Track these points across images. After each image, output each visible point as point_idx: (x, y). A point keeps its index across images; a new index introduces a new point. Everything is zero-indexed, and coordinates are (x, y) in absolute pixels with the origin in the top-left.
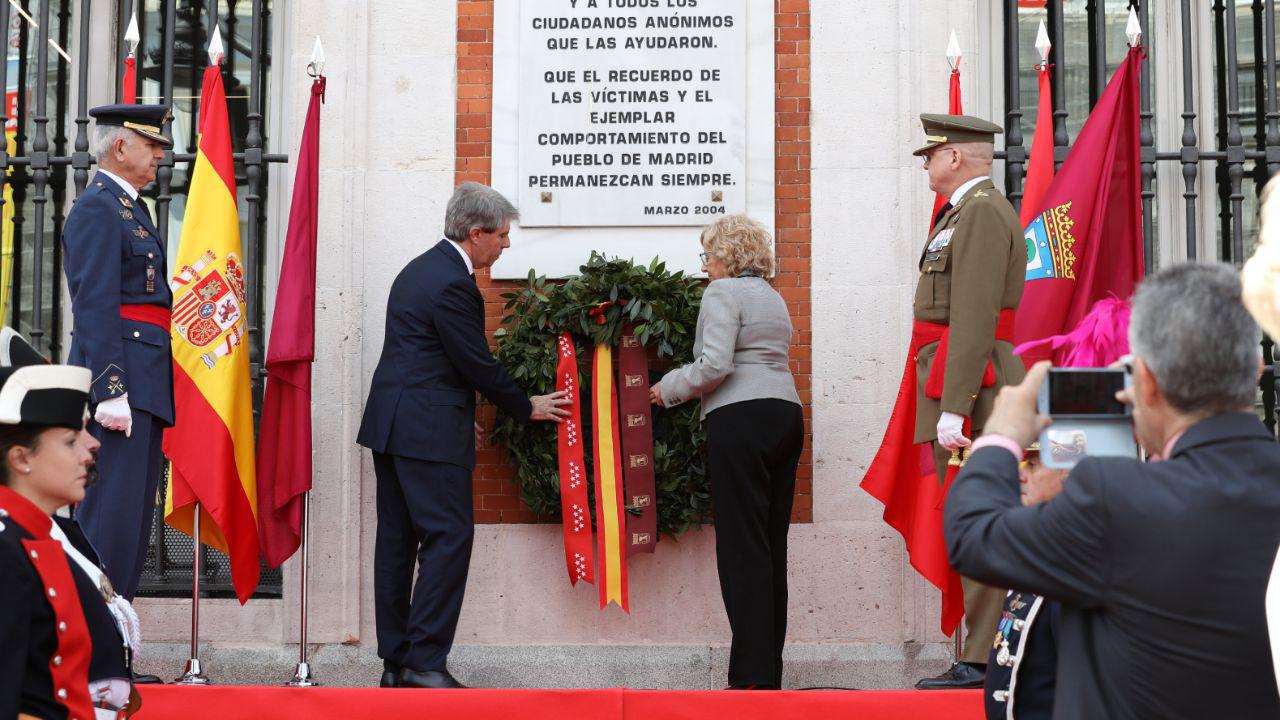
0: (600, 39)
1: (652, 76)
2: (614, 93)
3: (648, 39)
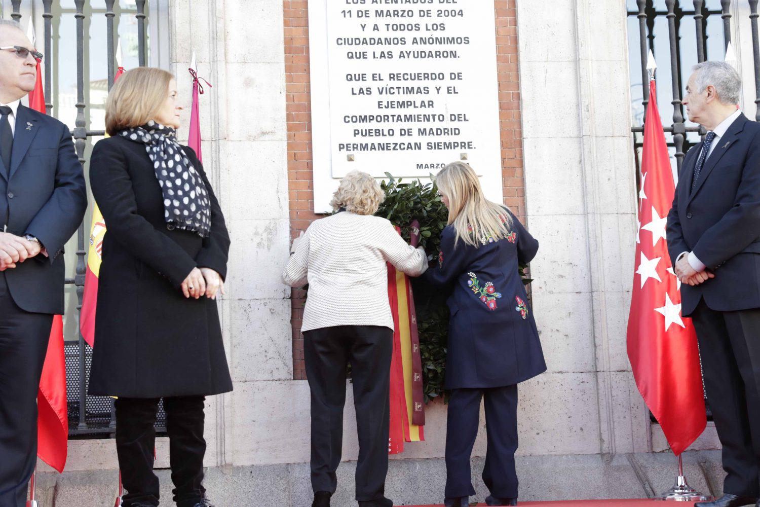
0: (383, 52)
1: (418, 76)
2: (393, 88)
3: (414, 52)
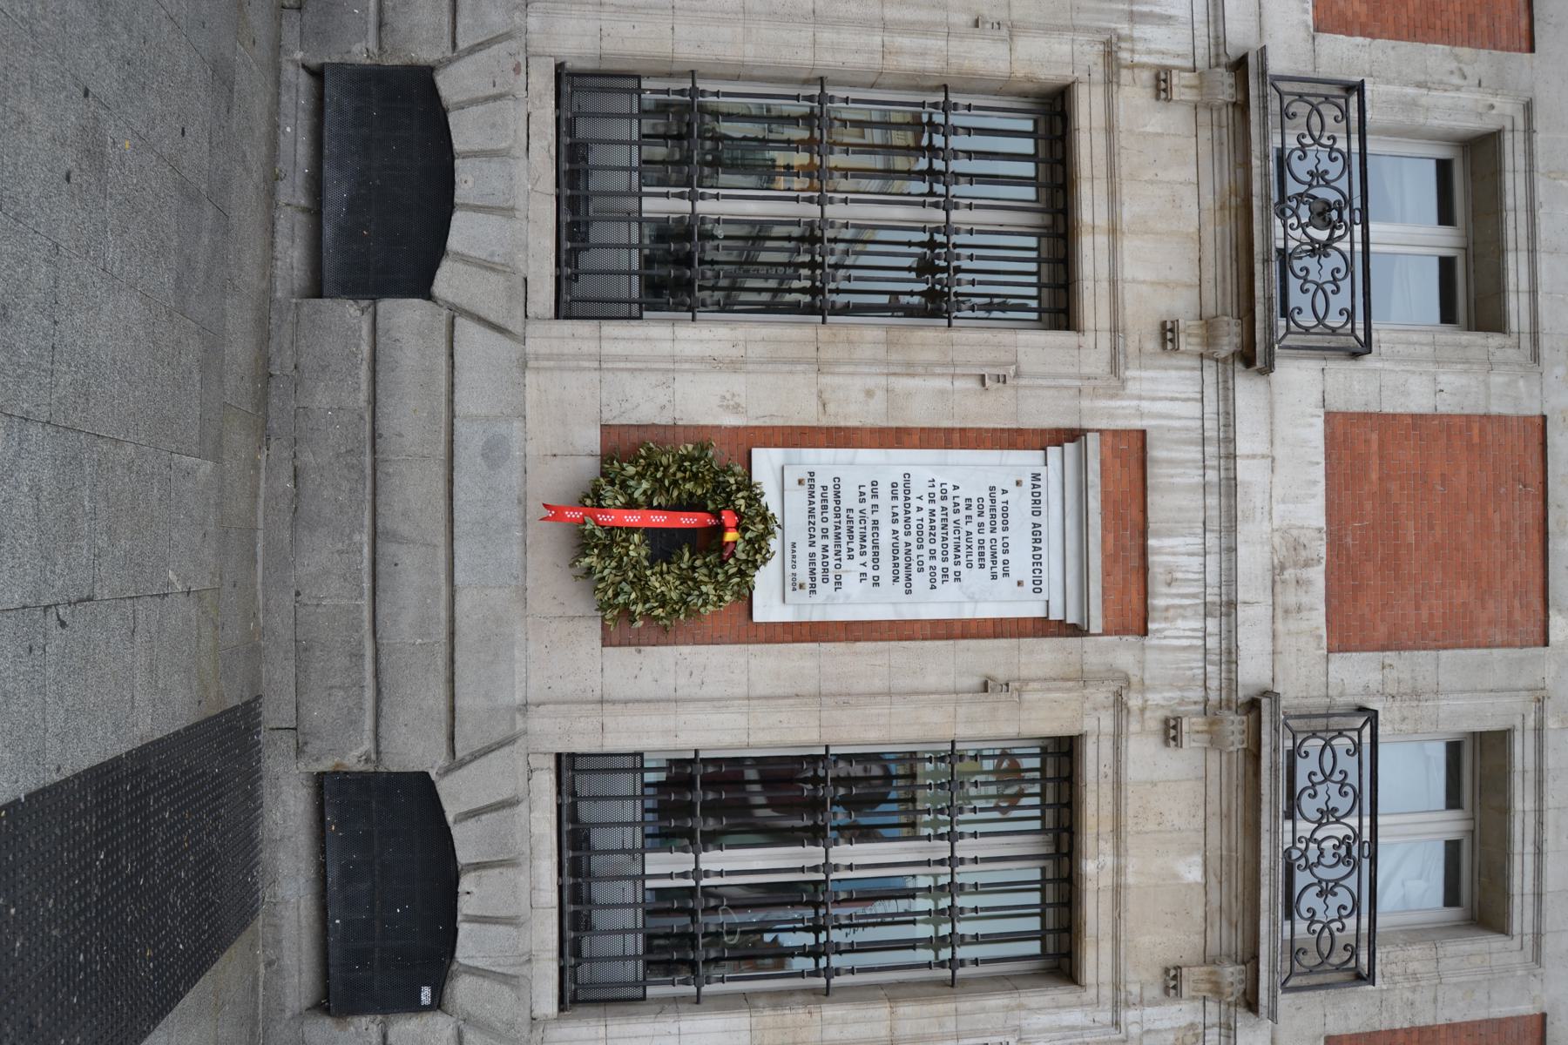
1: (876, 546)
